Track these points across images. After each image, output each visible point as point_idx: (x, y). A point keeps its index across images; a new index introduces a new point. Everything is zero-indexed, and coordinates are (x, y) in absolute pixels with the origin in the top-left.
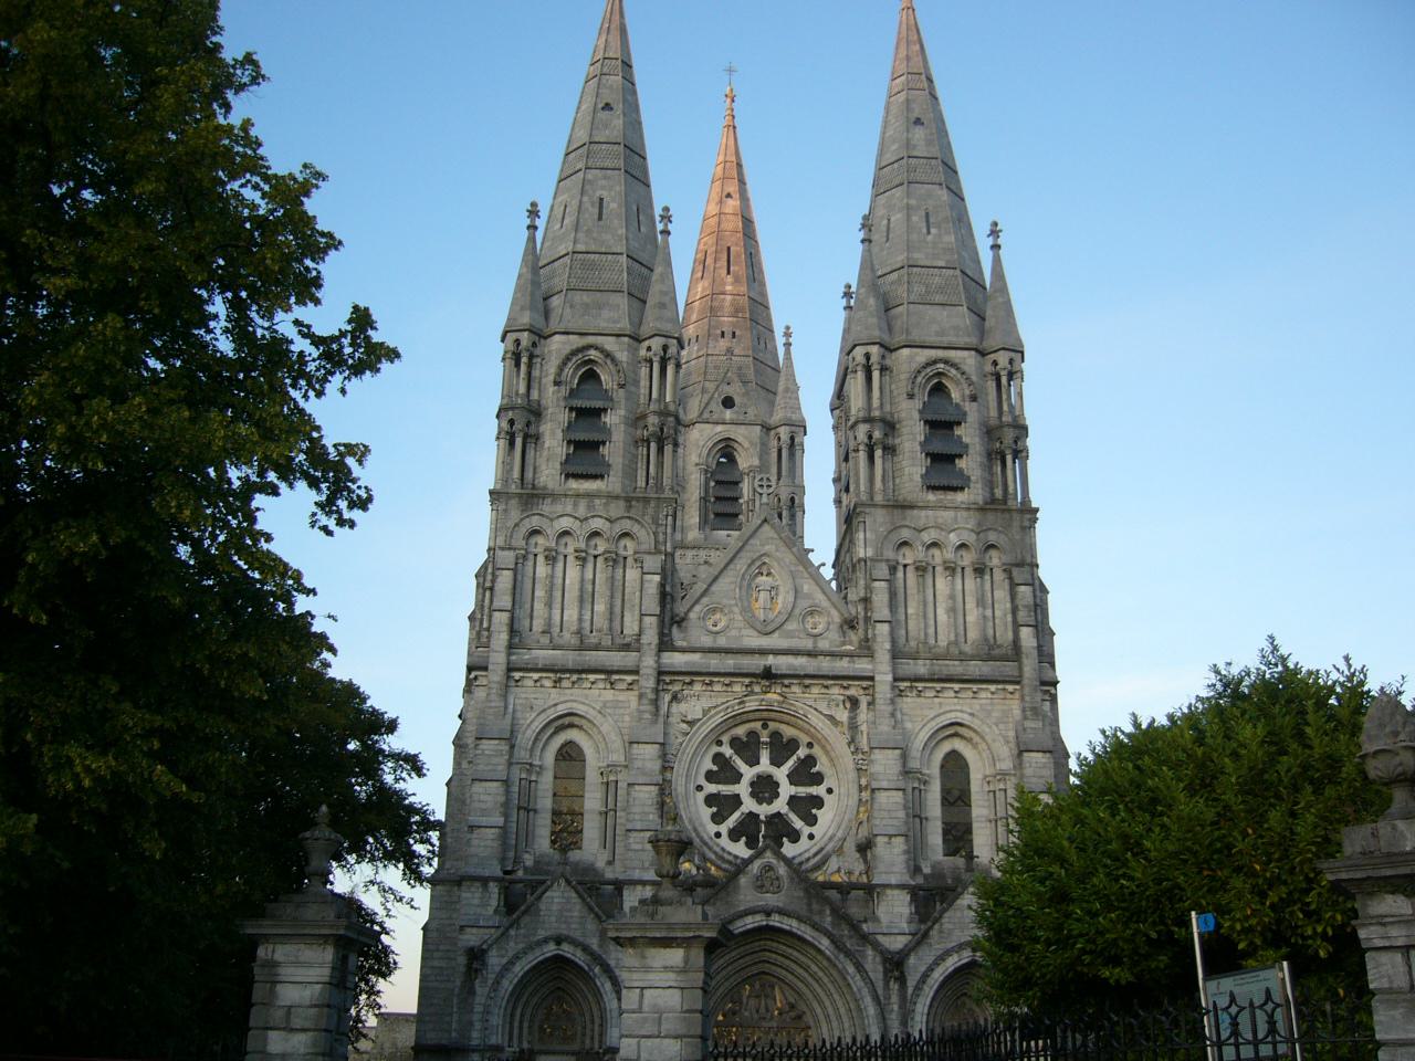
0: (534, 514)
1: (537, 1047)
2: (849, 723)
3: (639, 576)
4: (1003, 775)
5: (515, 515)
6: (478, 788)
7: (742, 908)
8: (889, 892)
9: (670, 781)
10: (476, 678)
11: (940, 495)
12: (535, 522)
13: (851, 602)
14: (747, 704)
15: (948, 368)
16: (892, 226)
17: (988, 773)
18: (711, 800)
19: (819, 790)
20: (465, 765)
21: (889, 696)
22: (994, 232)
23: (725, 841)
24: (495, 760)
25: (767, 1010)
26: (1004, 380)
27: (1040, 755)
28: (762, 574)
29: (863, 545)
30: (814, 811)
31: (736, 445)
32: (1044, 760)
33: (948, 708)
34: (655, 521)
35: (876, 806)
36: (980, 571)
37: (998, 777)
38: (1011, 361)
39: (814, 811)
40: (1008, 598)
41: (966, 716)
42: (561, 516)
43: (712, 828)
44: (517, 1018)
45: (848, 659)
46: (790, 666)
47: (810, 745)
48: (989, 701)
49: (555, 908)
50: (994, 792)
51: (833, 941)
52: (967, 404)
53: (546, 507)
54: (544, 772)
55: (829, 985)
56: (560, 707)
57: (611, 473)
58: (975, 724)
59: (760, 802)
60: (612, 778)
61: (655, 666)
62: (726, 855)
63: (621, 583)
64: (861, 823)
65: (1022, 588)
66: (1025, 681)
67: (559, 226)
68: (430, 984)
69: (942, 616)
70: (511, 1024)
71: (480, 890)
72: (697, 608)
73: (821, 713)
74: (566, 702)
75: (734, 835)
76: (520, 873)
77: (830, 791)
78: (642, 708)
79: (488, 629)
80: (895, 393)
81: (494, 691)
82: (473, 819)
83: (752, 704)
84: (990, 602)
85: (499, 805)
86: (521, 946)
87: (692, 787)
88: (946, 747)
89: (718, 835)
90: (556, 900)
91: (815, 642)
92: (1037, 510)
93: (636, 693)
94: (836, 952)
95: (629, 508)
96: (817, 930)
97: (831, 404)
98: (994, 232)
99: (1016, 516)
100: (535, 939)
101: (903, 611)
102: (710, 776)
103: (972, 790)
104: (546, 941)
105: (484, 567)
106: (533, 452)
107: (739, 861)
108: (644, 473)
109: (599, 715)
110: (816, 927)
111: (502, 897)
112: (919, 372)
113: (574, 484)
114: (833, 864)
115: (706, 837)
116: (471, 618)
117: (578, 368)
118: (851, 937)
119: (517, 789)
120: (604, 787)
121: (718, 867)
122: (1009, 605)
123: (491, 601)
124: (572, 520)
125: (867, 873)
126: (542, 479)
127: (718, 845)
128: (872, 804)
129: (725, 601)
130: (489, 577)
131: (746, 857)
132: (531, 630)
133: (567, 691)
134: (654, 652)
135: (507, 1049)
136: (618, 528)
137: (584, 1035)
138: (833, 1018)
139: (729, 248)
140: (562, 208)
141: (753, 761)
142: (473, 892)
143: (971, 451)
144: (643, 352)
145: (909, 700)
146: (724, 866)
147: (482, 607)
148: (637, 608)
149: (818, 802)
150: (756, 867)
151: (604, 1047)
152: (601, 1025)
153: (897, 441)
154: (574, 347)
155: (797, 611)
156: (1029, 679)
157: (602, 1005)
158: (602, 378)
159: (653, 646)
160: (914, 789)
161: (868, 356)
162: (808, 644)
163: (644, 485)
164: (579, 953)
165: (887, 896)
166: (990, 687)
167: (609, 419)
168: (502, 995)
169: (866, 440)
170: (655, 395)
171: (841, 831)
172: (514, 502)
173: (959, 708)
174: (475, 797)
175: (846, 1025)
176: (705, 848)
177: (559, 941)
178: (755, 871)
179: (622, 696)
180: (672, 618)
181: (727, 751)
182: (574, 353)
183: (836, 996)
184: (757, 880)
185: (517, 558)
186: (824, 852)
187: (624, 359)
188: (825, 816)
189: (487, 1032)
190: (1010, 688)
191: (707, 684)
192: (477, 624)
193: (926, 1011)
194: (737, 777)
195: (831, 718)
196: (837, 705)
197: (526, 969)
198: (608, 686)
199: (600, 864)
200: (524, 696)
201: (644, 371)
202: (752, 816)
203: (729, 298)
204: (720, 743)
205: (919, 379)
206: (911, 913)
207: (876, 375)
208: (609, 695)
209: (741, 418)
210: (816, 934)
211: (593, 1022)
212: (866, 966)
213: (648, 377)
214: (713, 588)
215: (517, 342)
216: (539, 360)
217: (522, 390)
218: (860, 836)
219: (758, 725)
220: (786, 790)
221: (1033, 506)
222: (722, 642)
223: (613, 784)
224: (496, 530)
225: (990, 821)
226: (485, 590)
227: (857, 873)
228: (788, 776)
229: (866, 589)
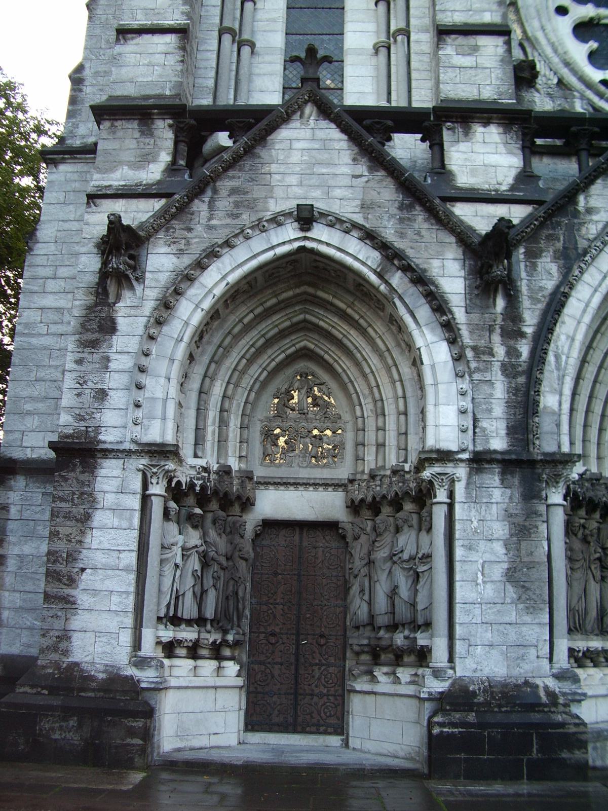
1: (260, 472)
68: (34, 341)
70: (201, 412)
71: (137, 135)
90: (297, 145)
104: (277, 221)
111: (183, 148)
189: (139, 413)
211: (381, 413)
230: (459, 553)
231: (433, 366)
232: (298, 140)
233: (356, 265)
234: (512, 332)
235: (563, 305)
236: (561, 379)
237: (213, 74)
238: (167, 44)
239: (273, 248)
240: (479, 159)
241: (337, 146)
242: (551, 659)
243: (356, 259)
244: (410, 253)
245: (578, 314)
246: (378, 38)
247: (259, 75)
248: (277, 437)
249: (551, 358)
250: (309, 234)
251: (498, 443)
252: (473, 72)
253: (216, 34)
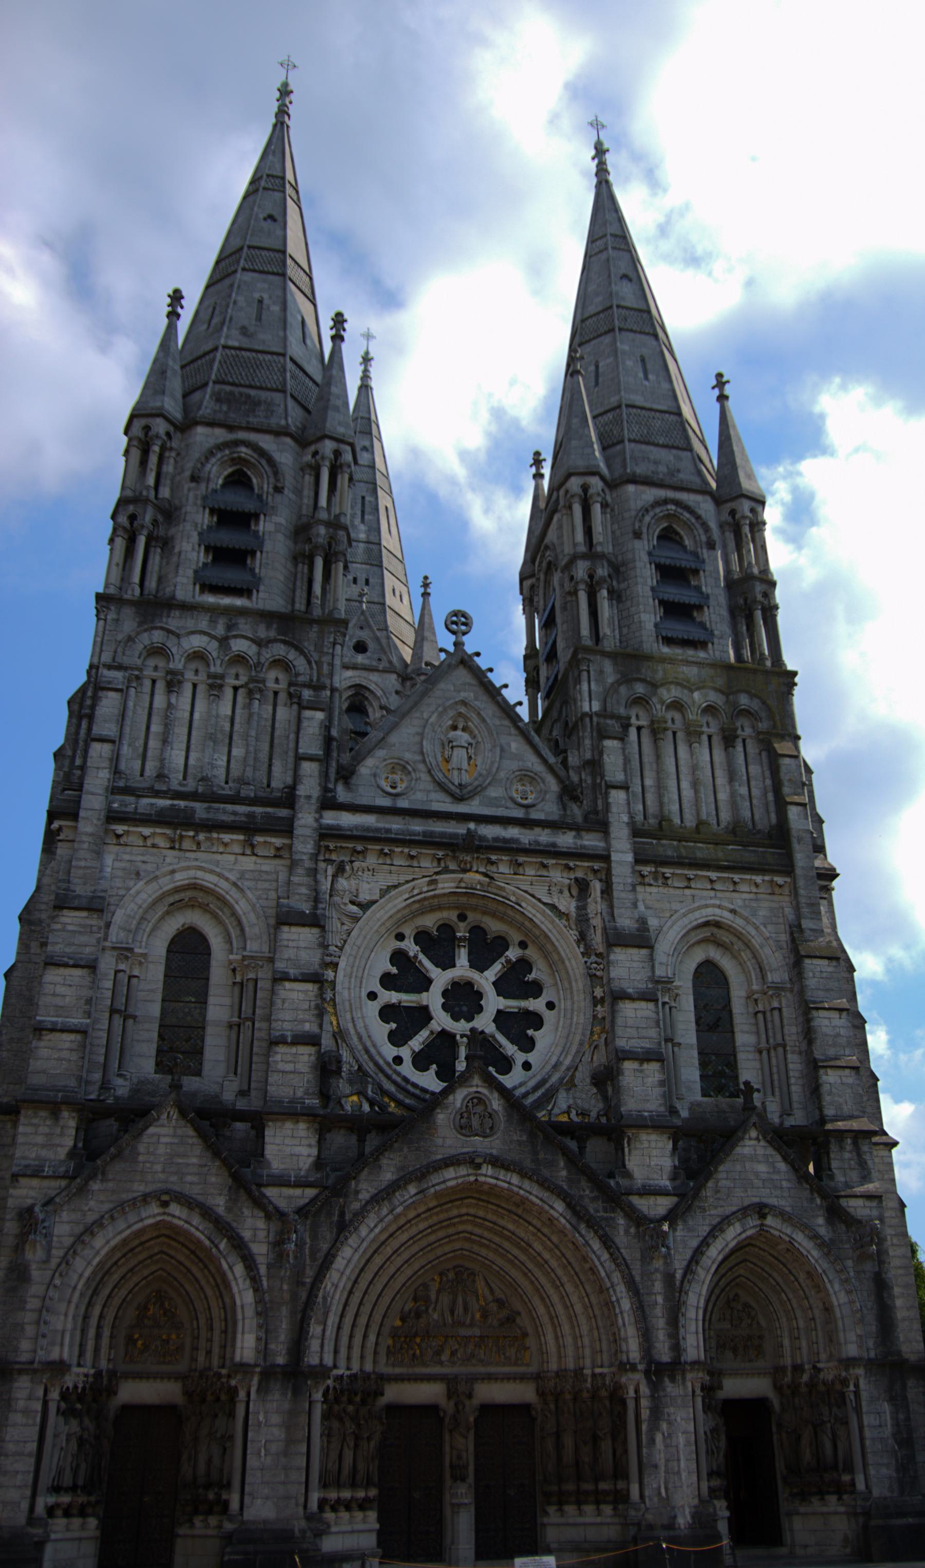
0: (156, 628)
2: (578, 915)
3: (295, 713)
4: (778, 989)
5: (129, 624)
6: (53, 976)
7: (439, 1157)
8: (644, 1136)
9: (333, 983)
10: (60, 829)
11: (677, 652)
12: (158, 636)
13: (573, 768)
14: (440, 885)
15: (679, 510)
16: (601, 370)
17: (755, 987)
18: (387, 1013)
19: (536, 1005)
20: (35, 947)
21: (629, 880)
22: (720, 382)
23: (407, 1069)
24: (83, 939)
25: (466, 1309)
26: (746, 529)
27: (825, 962)
28: (454, 728)
29: (587, 699)
30: (530, 1032)
31: (367, 694)
32: (830, 969)
33: (703, 902)
34: (319, 648)
35: (619, 1021)
36: (729, 740)
37: (770, 993)
38: (752, 510)
39: (530, 1032)
40: (767, 774)
41: (726, 914)
42: (193, 633)
43: (390, 1051)
44: (94, 1321)
45: (573, 833)
46: (496, 839)
47: (523, 945)
48: (752, 896)
49: (161, 1150)
50: (764, 1013)
51: (569, 1206)
52: (705, 551)
53: (174, 621)
54: (151, 966)
55: (560, 1272)
56: (178, 876)
57: (262, 588)
58: (738, 923)
59: (456, 1018)
60: (252, 975)
61: (315, 825)
62: (409, 1087)
63: (269, 723)
64: (596, 1047)
65: (787, 761)
66: (798, 871)
67: (205, 326)
69: (687, 793)
72: (370, 762)
73: (539, 900)
74: (188, 868)
75: (421, 1061)
76: (110, 1101)
77: (550, 1006)
78: (295, 879)
79: (83, 768)
80: (618, 533)
81: (86, 846)
82: (45, 1017)
83: (446, 884)
84: (745, 778)
85: (83, 1001)
86: (107, 1206)
87: (364, 994)
88: (699, 955)
89: (398, 1060)
90: (163, 1140)
91: (527, 813)
92: (795, 674)
93: (288, 862)
94: (574, 1221)
96: (548, 1189)
97: (521, 574)
98: (720, 382)
100: (131, 1196)
101: (639, 782)
102: (387, 981)
103: (734, 1011)
104: (145, 1198)
105: (83, 690)
106: (158, 558)
107: (428, 1096)
108: (305, 595)
109: (234, 889)
110: (544, 1183)
112: (647, 510)
113: (211, 599)
114: (562, 1101)
115: (381, 1062)
116: (58, 755)
118: (594, 1199)
119: (109, 984)
120: (237, 990)
121: (399, 1103)
122: (768, 782)
123: (90, 729)
124: (206, 639)
125: (606, 1115)
126: (168, 590)
127: (399, 1074)
128: (613, 1022)
129: (408, 756)
130: (89, 702)
131: (438, 1090)
132: (142, 775)
133: (188, 854)
134: (314, 807)
135: (75, 1370)
136: (268, 655)
137: (195, 1348)
138: (563, 1319)
139: (363, 498)
140: (211, 309)
141: (447, 963)
142: (36, 1126)
143: (712, 602)
144: (308, 458)
145: (654, 890)
146: (407, 1101)
147: (76, 741)
148: (291, 754)
149: (536, 1021)
150: (459, 1097)
151: (228, 1363)
152: (225, 1332)
153: (623, 586)
154: (221, 440)
155: (502, 774)
156: (803, 868)
157: (227, 1300)
158: (254, 481)
159: (313, 801)
160: (664, 1004)
161: (585, 488)
162: (519, 813)
163: (303, 608)
164: (196, 1220)
165: (641, 1142)
166: (754, 877)
167: (263, 526)
168: (73, 1283)
169: (586, 577)
170: (323, 502)
171: (570, 1058)
172: (128, 611)
173: (718, 902)
174: (49, 989)
175: (585, 1329)
176: (380, 1075)
177: (165, 1197)
178: (458, 1105)
179: (268, 866)
180: (338, 773)
181: (411, 948)
182: (220, 447)
183: (569, 1287)
184: (462, 1117)
185: (129, 681)
186: (547, 1085)
187: (283, 460)
188: (543, 1038)
190: (779, 880)
191: (386, 854)
192: (67, 762)
193: (702, 1304)
194: (425, 984)
195: (553, 907)
196: (561, 892)
197: (113, 1243)
198: (248, 852)
199: (228, 1096)
200: (127, 857)
201: (309, 479)
202: (445, 1037)
203: (362, 545)
204: (400, 937)
205: (647, 519)
206: (675, 1167)
207: (597, 509)
208: (248, 863)
209: (374, 663)
210: (545, 1195)
211: (211, 1329)
212: (617, 1240)
213: (312, 487)
214: (394, 738)
215: (147, 428)
216: (173, 454)
217: (151, 481)
218: (595, 1065)
219: (452, 915)
220: (493, 1002)
221: (790, 667)
222: (403, 803)
223: (251, 986)
224: (99, 645)
225: (760, 1052)
226: (80, 718)
227: (593, 1114)
228: (494, 983)
229: (593, 751)
230: (250, 1435)
231: (242, 1306)
232: (165, 1136)
233: (198, 1234)
234: (298, 1282)
235: (331, 1263)
236: (326, 1314)
237: (103, 1051)
238: (72, 1042)
239: (142, 1220)
240: (288, 1150)
241: (190, 1141)
242: (305, 1507)
243: (197, 1229)
244: (234, 1225)
245: (342, 1268)
246: (232, 1016)
247: (138, 1041)
248: (137, 1340)
249: (320, 1299)
250: (167, 1210)
251: (281, 1360)
252: (292, 1076)
253: (107, 1015)
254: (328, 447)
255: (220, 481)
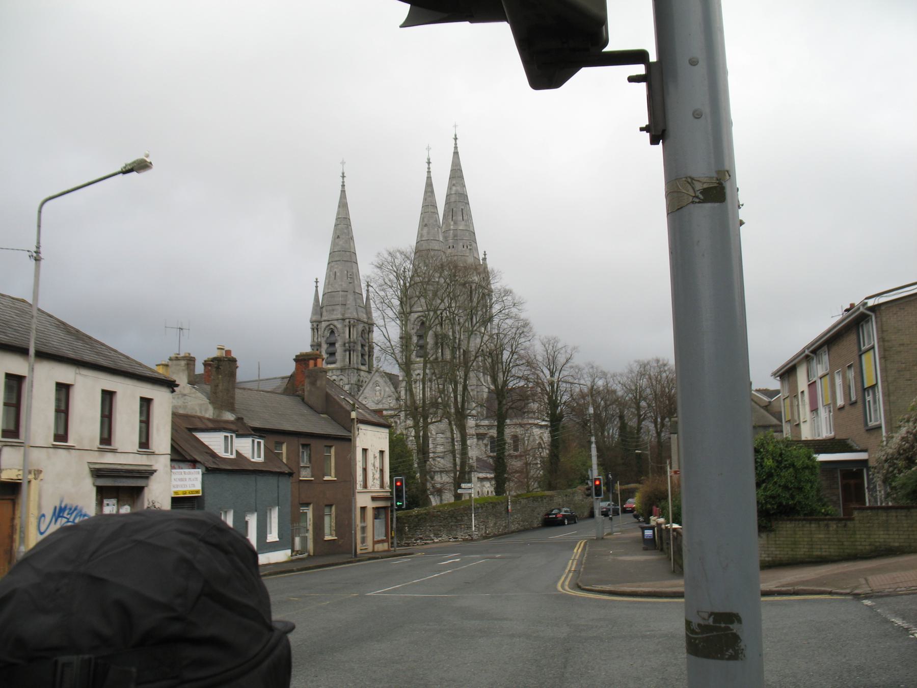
28: (377, 386)
34: (348, 375)
95: (341, 372)
99: (441, 363)
117: (328, 330)
155: (385, 396)
167: (337, 345)
254: (347, 320)
255: (329, 334)
